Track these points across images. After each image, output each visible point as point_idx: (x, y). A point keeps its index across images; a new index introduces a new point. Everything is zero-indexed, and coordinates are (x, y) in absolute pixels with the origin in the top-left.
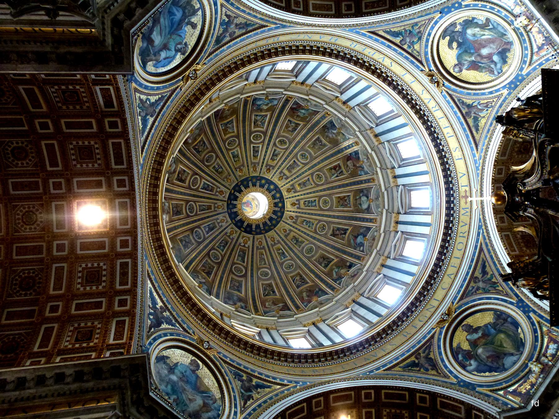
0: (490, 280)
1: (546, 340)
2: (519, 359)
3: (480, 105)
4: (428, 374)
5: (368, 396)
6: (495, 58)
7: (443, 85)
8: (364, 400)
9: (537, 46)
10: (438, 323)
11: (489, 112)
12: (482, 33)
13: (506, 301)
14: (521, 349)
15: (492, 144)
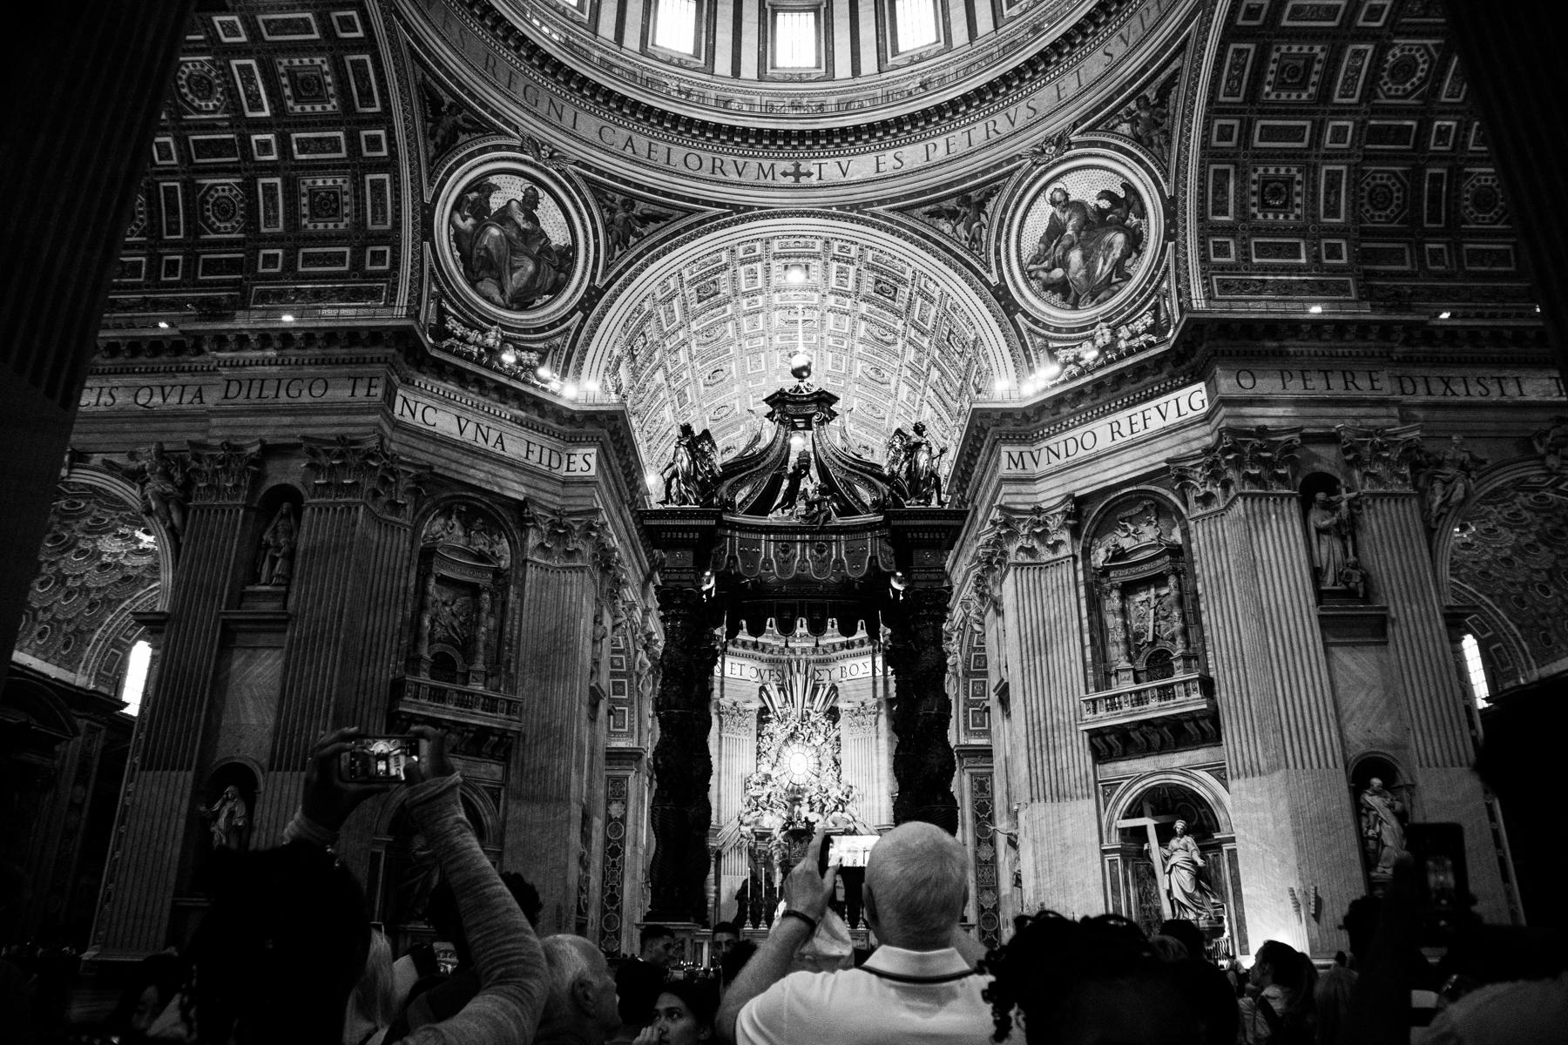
0: (632, 231)
1: (540, 345)
2: (497, 305)
3: (980, 227)
4: (425, 142)
5: (347, 24)
6: (1058, 273)
7: (1035, 164)
8: (334, 15)
9: (1057, 349)
10: (530, 138)
11: (963, 242)
12: (1110, 261)
13: (595, 266)
14: (515, 306)
15: (900, 241)
